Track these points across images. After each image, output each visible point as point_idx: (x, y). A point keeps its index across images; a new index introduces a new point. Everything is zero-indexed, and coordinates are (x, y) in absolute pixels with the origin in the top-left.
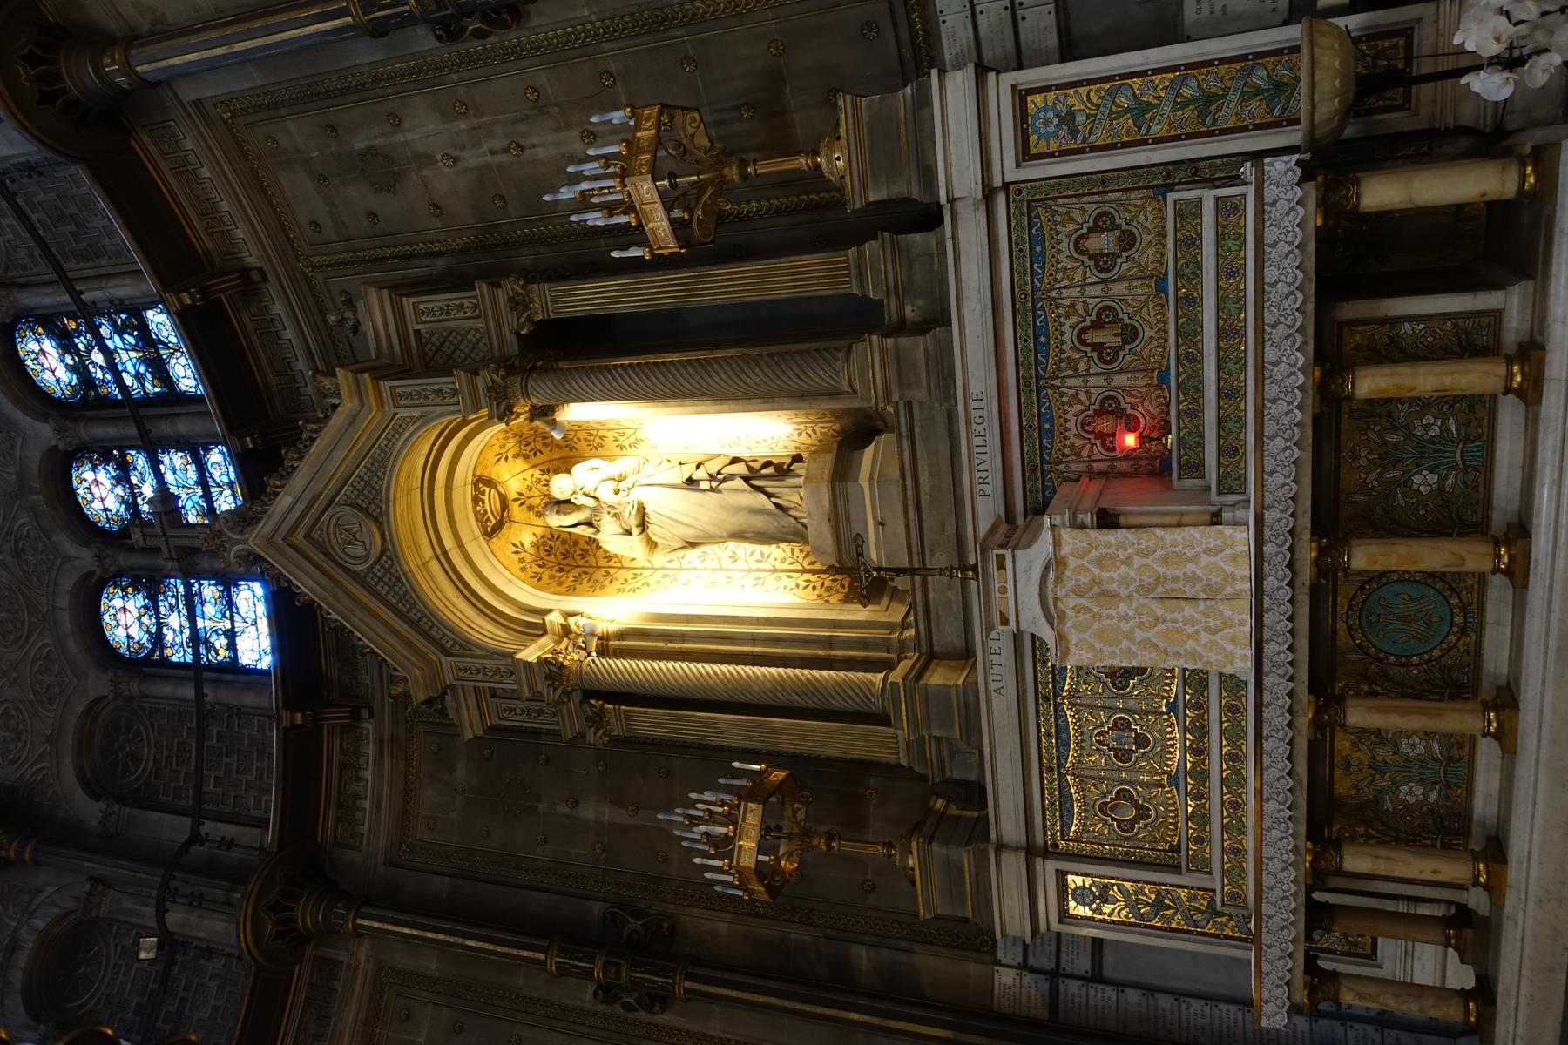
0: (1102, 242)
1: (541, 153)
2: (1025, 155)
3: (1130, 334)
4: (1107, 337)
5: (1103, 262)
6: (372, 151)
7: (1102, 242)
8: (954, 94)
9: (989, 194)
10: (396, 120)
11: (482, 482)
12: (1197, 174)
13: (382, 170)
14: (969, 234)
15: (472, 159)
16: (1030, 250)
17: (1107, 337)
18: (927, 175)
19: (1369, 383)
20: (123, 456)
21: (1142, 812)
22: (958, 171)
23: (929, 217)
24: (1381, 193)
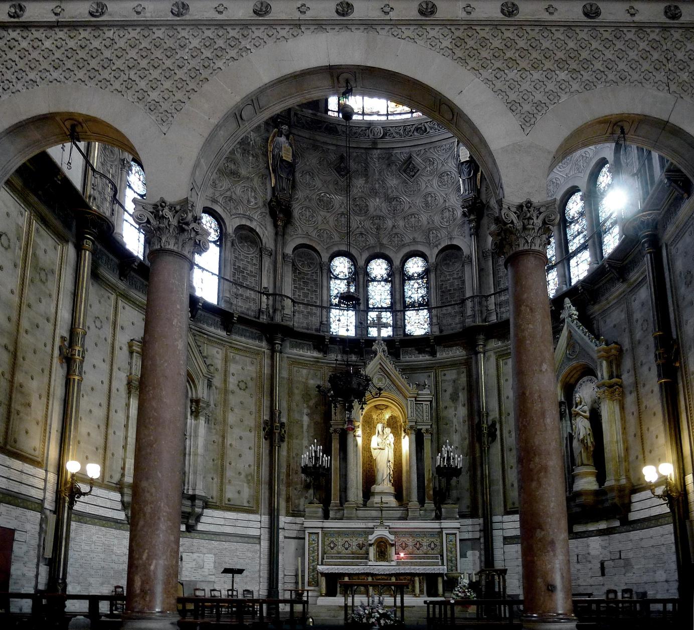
0: (433, 546)
1: (454, 436)
2: (447, 534)
3: (418, 549)
4: (418, 546)
5: (429, 545)
6: (458, 397)
7: (433, 546)
8: (456, 524)
9: (442, 528)
10: (464, 405)
11: (387, 407)
12: (442, 559)
13: (454, 398)
14: (435, 525)
15: (455, 420)
16: (432, 535)
17: (418, 546)
18: (445, 519)
19: (417, 579)
20: (389, 282)
21: (332, 548)
22: (446, 524)
23: (438, 517)
24: (440, 580)
